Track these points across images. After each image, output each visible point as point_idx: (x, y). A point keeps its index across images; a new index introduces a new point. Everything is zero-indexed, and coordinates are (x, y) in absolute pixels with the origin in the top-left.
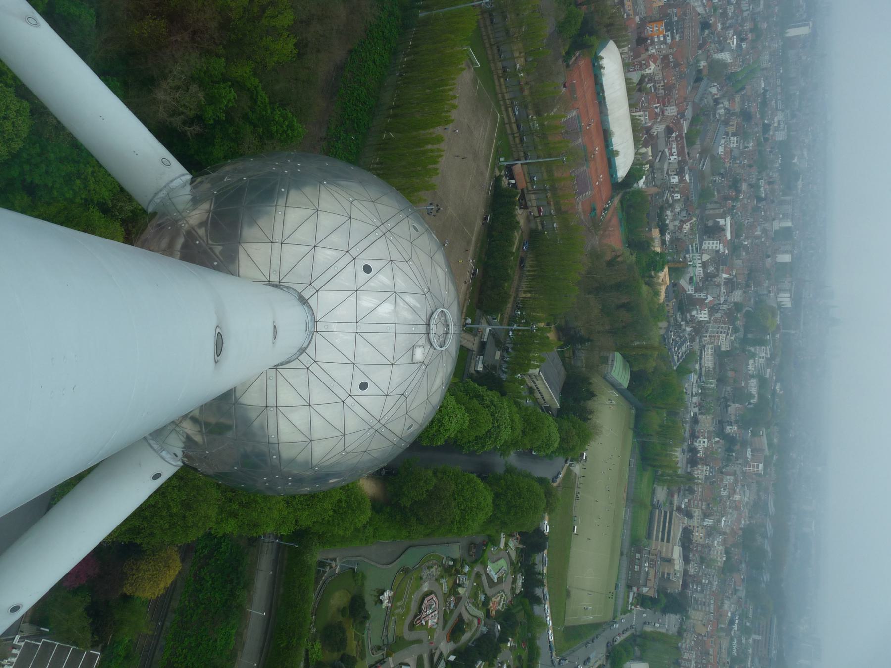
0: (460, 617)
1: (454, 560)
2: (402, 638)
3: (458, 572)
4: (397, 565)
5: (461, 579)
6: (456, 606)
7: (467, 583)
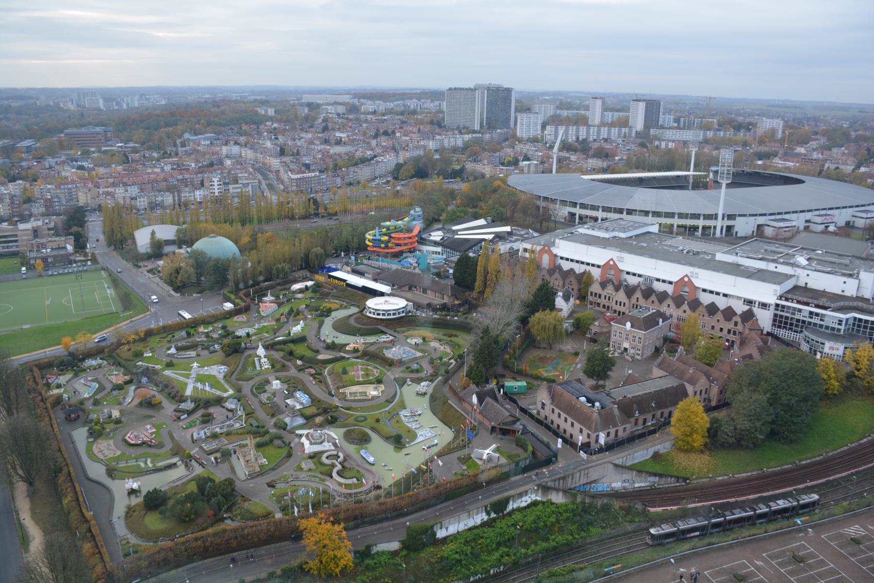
0: (141, 405)
7: (106, 410)
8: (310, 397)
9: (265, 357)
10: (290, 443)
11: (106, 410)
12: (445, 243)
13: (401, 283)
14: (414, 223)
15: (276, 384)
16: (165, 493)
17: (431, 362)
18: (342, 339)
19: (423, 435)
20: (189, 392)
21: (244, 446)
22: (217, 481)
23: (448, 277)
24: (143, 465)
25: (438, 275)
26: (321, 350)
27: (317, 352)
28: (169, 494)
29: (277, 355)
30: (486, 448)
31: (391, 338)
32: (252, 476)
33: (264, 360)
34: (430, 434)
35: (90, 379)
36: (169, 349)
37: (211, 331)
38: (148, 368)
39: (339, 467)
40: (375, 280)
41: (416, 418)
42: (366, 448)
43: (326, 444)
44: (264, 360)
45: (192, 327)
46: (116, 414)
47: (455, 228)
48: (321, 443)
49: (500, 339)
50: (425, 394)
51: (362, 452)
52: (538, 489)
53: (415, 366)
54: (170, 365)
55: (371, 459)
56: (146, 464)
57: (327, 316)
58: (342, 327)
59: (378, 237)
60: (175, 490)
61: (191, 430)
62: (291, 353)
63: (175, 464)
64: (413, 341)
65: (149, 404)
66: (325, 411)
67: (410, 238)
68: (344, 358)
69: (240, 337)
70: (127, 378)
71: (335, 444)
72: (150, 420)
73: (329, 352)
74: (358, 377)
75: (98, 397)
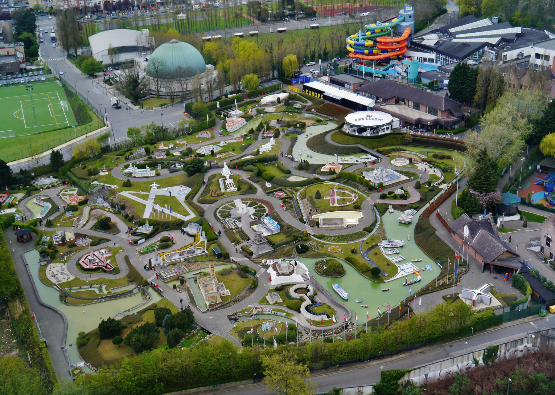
0: (95, 228)
2: (129, 276)
3: (51, 246)
4: (62, 308)
5: (56, 241)
6: (84, 236)
7: (59, 233)
8: (279, 224)
9: (231, 177)
10: (255, 273)
11: (59, 233)
12: (440, 49)
13: (386, 94)
14: (404, 24)
15: (242, 208)
16: (119, 322)
17: (418, 186)
18: (316, 158)
19: (406, 269)
20: (147, 215)
21: (205, 274)
22: (174, 312)
23: (442, 89)
24: (97, 291)
25: (431, 86)
26: (293, 171)
27: (289, 173)
28: (124, 323)
29: (245, 176)
30: (476, 287)
31: (373, 158)
32: (213, 307)
33: (229, 181)
34: (412, 267)
35: (43, 198)
36: (126, 167)
37: (172, 149)
38: (104, 187)
39: (308, 302)
41: (397, 251)
42: (339, 283)
44: (229, 181)
45: (151, 144)
46: (70, 236)
47: (452, 30)
48: (290, 274)
49: (500, 163)
50: (409, 223)
51: (335, 287)
53: (399, 192)
54: (127, 185)
55: (345, 295)
56: (101, 290)
57: (301, 133)
58: (317, 144)
59: (361, 42)
60: (130, 320)
61: (147, 257)
62: (259, 174)
63: (131, 292)
64: (401, 163)
65: (105, 225)
66: (296, 239)
67: (398, 42)
68: (318, 180)
69: (204, 155)
70: (82, 198)
71: (304, 276)
73: (303, 172)
74: (334, 202)
75: (51, 218)
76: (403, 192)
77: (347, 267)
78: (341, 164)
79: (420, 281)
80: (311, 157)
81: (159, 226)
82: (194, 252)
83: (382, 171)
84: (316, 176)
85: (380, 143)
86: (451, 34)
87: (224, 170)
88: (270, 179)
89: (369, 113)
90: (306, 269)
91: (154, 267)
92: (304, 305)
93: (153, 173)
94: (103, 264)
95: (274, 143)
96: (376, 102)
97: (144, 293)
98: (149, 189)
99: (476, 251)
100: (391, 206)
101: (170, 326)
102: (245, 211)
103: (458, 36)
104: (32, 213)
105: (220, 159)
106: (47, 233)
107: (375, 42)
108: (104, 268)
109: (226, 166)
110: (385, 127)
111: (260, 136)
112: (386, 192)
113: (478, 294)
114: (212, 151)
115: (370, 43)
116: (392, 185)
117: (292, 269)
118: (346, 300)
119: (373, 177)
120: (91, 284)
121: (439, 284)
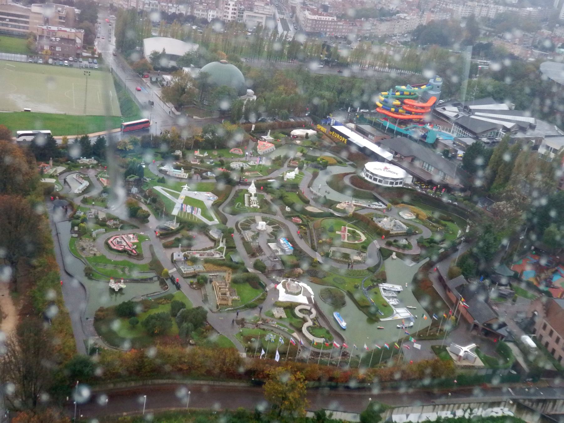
1: (73, 226)
2: (151, 264)
7: (93, 211)
8: (293, 247)
14: (431, 92)
15: (262, 225)
18: (334, 195)
20: (175, 212)
26: (312, 202)
27: (307, 202)
30: (465, 344)
39: (310, 323)
40: (378, 144)
43: (301, 295)
48: (297, 294)
51: (335, 315)
52: (513, 405)
54: (162, 181)
55: (343, 324)
63: (151, 279)
67: (423, 108)
68: (332, 215)
71: (309, 299)
72: (136, 231)
76: (407, 243)
77: (347, 299)
78: (355, 205)
79: (412, 327)
80: (329, 193)
81: (186, 224)
82: (213, 255)
83: (391, 220)
84: (331, 211)
85: (395, 194)
86: (470, 110)
87: (251, 187)
88: (291, 205)
89: (388, 165)
90: (312, 293)
91: (175, 261)
92: (306, 325)
93: (186, 176)
94: (129, 248)
95: (297, 173)
96: (394, 157)
97: (163, 283)
98: (180, 190)
99: (467, 311)
100: (394, 253)
101: (184, 318)
102: (264, 228)
103: (476, 113)
104: (70, 187)
105: (248, 177)
106: (82, 209)
107: (403, 103)
108: (130, 252)
109: (253, 184)
110: (399, 181)
111: (286, 165)
112: (392, 240)
113: (465, 351)
114: (242, 168)
115: (398, 103)
116: (397, 235)
117: (299, 290)
118: (344, 330)
119: (385, 223)
120: (116, 264)
121: (430, 333)
